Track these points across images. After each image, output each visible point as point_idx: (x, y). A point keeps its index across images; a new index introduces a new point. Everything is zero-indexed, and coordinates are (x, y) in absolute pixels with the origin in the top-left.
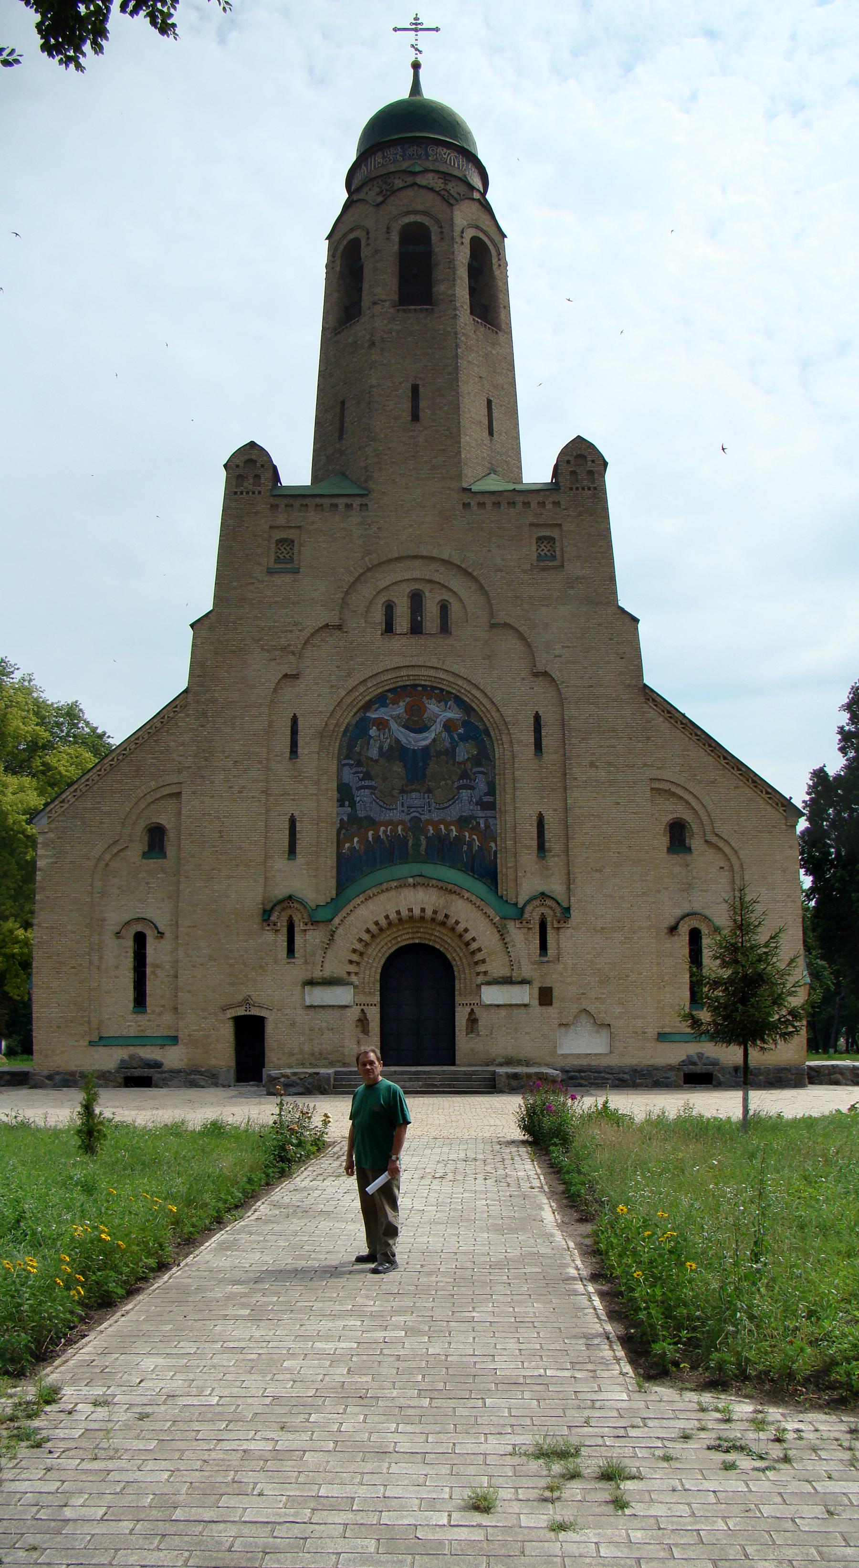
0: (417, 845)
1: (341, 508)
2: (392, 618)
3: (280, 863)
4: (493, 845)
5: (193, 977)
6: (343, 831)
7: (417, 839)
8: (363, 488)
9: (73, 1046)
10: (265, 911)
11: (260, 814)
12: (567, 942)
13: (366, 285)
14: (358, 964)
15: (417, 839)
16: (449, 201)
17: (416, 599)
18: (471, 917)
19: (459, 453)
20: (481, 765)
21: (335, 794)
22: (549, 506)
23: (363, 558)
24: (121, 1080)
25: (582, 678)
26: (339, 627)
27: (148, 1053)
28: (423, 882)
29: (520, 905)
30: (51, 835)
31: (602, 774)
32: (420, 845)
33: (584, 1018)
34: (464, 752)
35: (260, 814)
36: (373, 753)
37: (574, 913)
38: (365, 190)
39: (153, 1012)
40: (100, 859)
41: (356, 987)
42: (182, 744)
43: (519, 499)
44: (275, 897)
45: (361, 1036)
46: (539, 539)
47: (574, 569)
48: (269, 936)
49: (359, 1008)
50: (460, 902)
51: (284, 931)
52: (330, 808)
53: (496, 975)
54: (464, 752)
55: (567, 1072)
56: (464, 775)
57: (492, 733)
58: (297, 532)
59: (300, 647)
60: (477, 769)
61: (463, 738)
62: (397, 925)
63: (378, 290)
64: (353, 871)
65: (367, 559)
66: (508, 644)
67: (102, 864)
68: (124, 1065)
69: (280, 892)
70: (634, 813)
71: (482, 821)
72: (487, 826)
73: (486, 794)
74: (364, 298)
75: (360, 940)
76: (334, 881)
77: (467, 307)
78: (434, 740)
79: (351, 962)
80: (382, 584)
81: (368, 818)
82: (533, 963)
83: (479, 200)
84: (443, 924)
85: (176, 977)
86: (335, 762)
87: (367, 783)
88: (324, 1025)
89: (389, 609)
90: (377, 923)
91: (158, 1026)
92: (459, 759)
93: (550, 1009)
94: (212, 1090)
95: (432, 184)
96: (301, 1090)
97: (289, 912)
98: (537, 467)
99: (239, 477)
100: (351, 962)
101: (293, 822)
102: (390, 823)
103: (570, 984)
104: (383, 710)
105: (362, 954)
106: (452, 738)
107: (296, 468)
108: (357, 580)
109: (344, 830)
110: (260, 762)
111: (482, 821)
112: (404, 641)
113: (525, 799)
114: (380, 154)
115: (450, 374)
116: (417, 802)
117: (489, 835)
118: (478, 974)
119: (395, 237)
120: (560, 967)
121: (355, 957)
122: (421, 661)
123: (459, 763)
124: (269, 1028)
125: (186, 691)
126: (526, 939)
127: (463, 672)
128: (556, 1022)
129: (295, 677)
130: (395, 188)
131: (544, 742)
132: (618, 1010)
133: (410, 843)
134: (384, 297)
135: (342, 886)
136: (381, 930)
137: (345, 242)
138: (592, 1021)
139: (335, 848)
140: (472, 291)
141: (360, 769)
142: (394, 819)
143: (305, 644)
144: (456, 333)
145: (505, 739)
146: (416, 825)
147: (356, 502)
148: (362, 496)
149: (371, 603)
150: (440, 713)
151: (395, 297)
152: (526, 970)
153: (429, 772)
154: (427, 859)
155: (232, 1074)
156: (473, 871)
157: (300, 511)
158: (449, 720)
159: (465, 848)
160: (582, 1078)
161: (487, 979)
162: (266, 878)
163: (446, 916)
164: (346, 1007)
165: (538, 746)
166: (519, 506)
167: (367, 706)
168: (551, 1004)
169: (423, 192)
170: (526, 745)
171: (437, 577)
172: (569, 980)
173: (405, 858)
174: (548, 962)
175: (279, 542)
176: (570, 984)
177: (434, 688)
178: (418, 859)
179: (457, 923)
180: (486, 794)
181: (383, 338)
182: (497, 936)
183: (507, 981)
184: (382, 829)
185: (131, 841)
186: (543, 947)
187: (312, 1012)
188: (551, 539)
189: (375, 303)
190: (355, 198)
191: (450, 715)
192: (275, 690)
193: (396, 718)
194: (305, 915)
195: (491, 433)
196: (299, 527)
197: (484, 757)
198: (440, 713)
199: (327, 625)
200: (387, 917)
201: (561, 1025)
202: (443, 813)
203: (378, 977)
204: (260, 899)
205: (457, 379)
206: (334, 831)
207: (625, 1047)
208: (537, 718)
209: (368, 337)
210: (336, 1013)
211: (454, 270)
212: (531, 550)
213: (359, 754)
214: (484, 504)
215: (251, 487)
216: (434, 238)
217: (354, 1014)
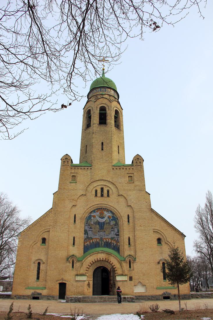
0: (102, 244)
1: (86, 169)
2: (97, 193)
3: (71, 247)
4: (119, 244)
5: (51, 273)
6: (85, 240)
7: (102, 242)
8: (90, 165)
9: (22, 289)
10: (67, 258)
11: (67, 236)
12: (135, 266)
13: (92, 120)
14: (88, 271)
15: (102, 242)
16: (110, 101)
17: (102, 189)
18: (114, 261)
19: (112, 157)
20: (116, 226)
21: (84, 232)
22: (131, 169)
23: (91, 180)
24: (32, 298)
25: (138, 207)
26: (85, 195)
27: (39, 291)
28: (103, 252)
29: (125, 257)
30: (21, 239)
31: (143, 228)
32: (102, 244)
33: (139, 284)
34: (113, 223)
35: (67, 236)
36: (92, 223)
37: (137, 259)
38: (92, 98)
39: (41, 281)
40: (31, 245)
41: (87, 276)
42: (50, 220)
43: (125, 168)
44: (70, 255)
45: (88, 288)
46: (129, 176)
47: (136, 183)
48: (68, 264)
49: (88, 281)
50: (112, 257)
51: (72, 263)
53: (119, 274)
54: (113, 223)
55: (136, 297)
56: (112, 228)
57: (118, 219)
58: (76, 174)
59: (77, 199)
60: (115, 227)
61: (112, 220)
62: (97, 262)
63: (95, 121)
65: (91, 180)
66: (122, 199)
67: (32, 246)
68: (33, 294)
69: (71, 254)
70: (150, 237)
71: (116, 238)
72: (117, 240)
73: (117, 232)
74: (91, 123)
75: (89, 265)
76: (83, 252)
77: (114, 125)
78: (106, 220)
79: (86, 270)
81: (91, 237)
82: (128, 271)
83: (117, 101)
84: (107, 262)
85: (47, 273)
86: (84, 225)
87: (91, 230)
88: (80, 285)
89: (96, 191)
90: (92, 261)
91: (42, 284)
93: (132, 282)
94: (53, 301)
95: (107, 97)
96: (75, 301)
97: (72, 259)
98: (128, 161)
99: (64, 162)
100: (86, 270)
101: (74, 238)
102: (96, 239)
103: (136, 276)
104: (94, 213)
105: (89, 268)
106: (110, 220)
107: (76, 161)
108: (89, 184)
109: (86, 240)
110: (67, 224)
111: (116, 238)
112: (99, 198)
113: (126, 233)
114: (95, 90)
115: (110, 140)
116: (102, 234)
117: (118, 241)
118: (115, 273)
119: (99, 109)
120: (134, 272)
121: (87, 269)
123: (111, 226)
124: (67, 286)
125: (52, 208)
126: (126, 265)
127: (112, 205)
128: (133, 285)
129: (75, 206)
130: (98, 98)
131: (130, 221)
132: (147, 281)
133: (100, 243)
134: (96, 123)
135: (84, 252)
136: (93, 263)
137: (87, 110)
138: (141, 284)
139: (83, 244)
140: (115, 121)
141: (89, 226)
142: (97, 238)
143: (78, 198)
144: (112, 131)
145: (121, 220)
146: (101, 239)
147: (89, 168)
148: (91, 166)
149: (92, 190)
150: (107, 214)
151: (99, 123)
152: (126, 272)
153: (104, 227)
154: (104, 247)
155: (58, 297)
156: (114, 250)
157: (77, 169)
158: (109, 216)
159: (112, 244)
160: (140, 298)
161: (117, 274)
162: (68, 251)
163: (108, 260)
164: (85, 281)
165: (129, 221)
166: (125, 169)
167: (91, 212)
168: (132, 280)
169: (105, 99)
170: (126, 222)
171: (107, 184)
172: (136, 275)
173: (99, 247)
174: (131, 270)
175: (72, 176)
176: (136, 276)
177: (106, 209)
178: (102, 247)
179: (111, 261)
180: (117, 232)
181: (95, 132)
183: (122, 275)
184: (94, 240)
185: (39, 241)
186: (130, 267)
187: (77, 282)
188: (132, 176)
189: (94, 124)
190: (89, 100)
191: (109, 215)
192: (71, 208)
193: (97, 215)
194: (76, 259)
195: (119, 153)
196: (77, 173)
197: (117, 224)
198: (107, 214)
199: (83, 194)
200: (95, 260)
201: (134, 285)
202: (108, 236)
204: (66, 255)
205: (112, 141)
206: (83, 240)
207: (149, 291)
208: (128, 216)
209: (92, 131)
210: (83, 282)
211: (111, 117)
212: (127, 179)
213: (89, 223)
214: (117, 169)
215: (66, 164)
216: (107, 110)
217: (87, 283)
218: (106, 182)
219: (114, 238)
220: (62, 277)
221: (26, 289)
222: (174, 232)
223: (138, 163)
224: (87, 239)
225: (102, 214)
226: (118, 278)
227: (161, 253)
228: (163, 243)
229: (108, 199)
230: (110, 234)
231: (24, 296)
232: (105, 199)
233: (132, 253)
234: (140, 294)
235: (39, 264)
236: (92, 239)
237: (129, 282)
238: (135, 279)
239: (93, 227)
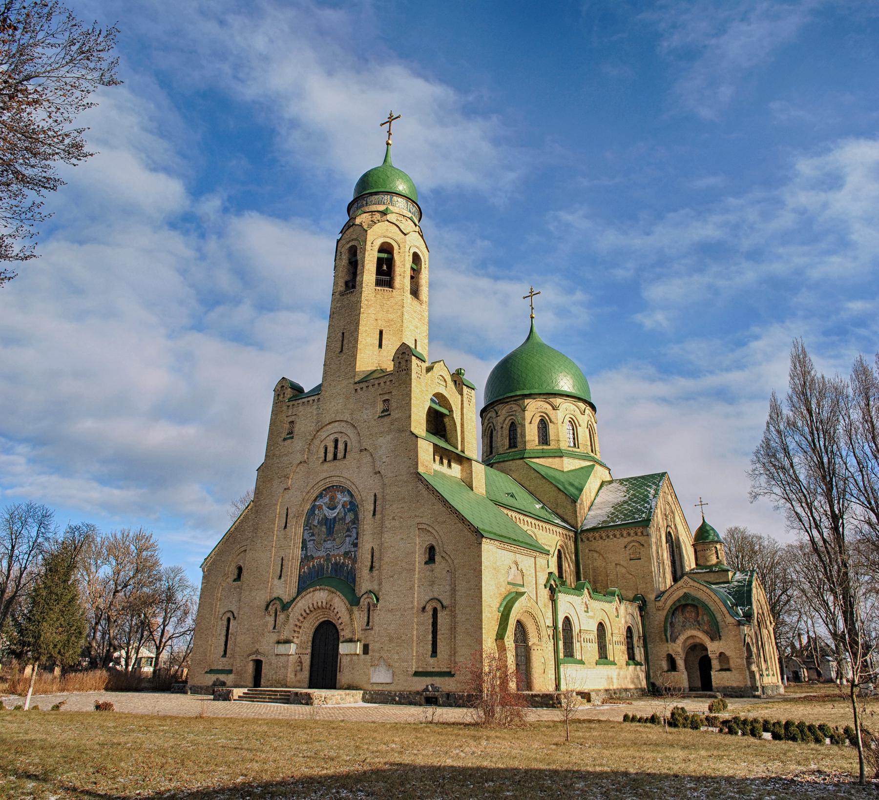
0: (328, 568)
3: (276, 581)
17: (336, 441)
22: (388, 383)
31: (396, 523)
36: (316, 523)
46: (384, 401)
47: (395, 414)
52: (298, 553)
54: (350, 517)
56: (348, 530)
64: (305, 584)
69: (275, 595)
80: (323, 438)
92: (347, 522)
93: (368, 657)
116: (329, 546)
117: (354, 561)
120: (373, 632)
121: (296, 629)
122: (333, 474)
132: (396, 657)
167: (315, 500)
171: (344, 430)
182: (348, 616)
183: (351, 641)
197: (356, 521)
198: (342, 498)
203: (311, 639)
208: (375, 495)
210: (285, 658)
218: (343, 424)
219: (350, 552)
220: (257, 647)
221: (206, 672)
223: (403, 363)
225: (332, 499)
226: (343, 648)
227: (432, 583)
228: (437, 558)
230: (343, 543)
232: (341, 462)
233: (375, 587)
234: (380, 688)
235: (229, 620)
236: (313, 558)
237: (363, 657)
238: (373, 651)
239: (316, 531)
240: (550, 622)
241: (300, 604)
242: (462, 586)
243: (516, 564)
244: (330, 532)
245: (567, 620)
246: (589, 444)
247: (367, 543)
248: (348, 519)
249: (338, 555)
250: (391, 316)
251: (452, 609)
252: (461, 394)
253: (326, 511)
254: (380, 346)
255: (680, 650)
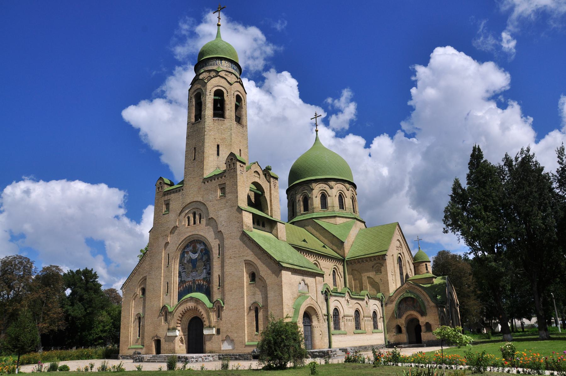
31: (232, 261)
36: (185, 262)
47: (229, 196)
54: (205, 258)
61: (205, 254)
93: (220, 336)
102: (189, 281)
116: (194, 275)
132: (236, 335)
150: (200, 247)
158: (202, 249)
167: (184, 249)
188: (224, 188)
198: (200, 247)
222: (269, 260)
224: (181, 282)
225: (194, 247)
226: (206, 332)
228: (257, 279)
229: (201, 225)
231: (127, 356)
239: (186, 266)
240: (325, 312)
241: (180, 308)
242: (271, 295)
243: (303, 280)
244: (194, 266)
245: (336, 310)
246: (352, 207)
247: (216, 272)
248: (204, 259)
249: (200, 280)
250: (224, 136)
251: (265, 307)
252: (269, 182)
253: (191, 254)
254: (218, 154)
255: (403, 322)
